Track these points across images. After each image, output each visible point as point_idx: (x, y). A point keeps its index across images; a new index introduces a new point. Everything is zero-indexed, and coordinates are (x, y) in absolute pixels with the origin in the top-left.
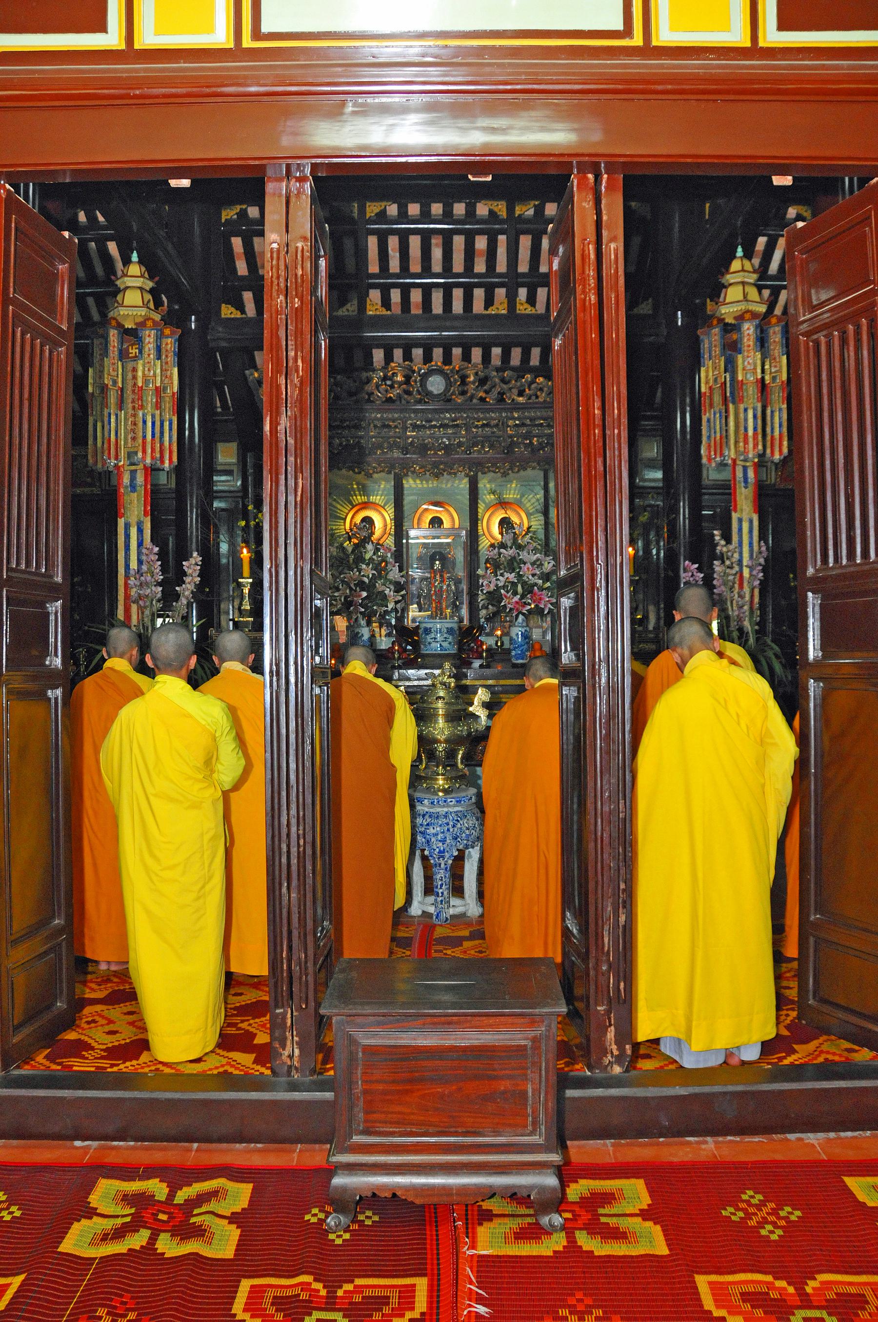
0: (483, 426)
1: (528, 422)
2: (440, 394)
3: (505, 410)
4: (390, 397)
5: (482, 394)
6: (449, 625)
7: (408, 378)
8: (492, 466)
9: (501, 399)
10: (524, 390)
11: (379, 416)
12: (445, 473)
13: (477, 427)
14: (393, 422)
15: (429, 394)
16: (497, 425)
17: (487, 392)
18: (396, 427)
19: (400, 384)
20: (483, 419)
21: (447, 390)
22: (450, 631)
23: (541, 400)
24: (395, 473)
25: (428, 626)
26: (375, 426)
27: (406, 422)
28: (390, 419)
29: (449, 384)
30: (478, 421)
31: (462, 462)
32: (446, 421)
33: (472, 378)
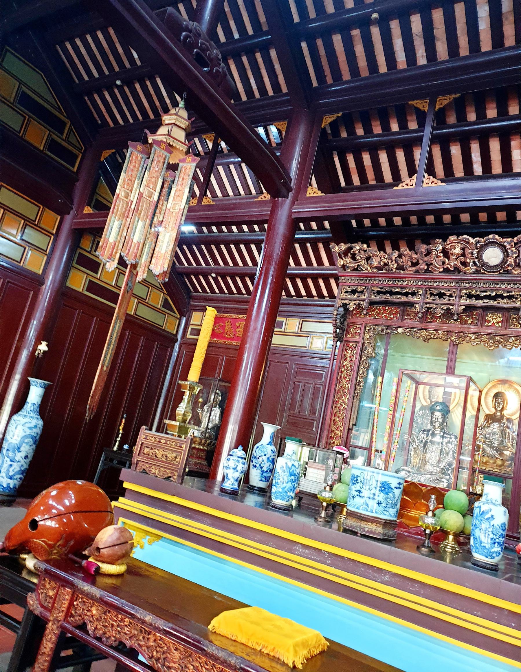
2: (497, 266)
4: (448, 268)
11: (435, 284)
12: (500, 346)
15: (484, 265)
18: (451, 296)
21: (504, 261)
26: (432, 294)
27: (461, 291)
29: (506, 254)
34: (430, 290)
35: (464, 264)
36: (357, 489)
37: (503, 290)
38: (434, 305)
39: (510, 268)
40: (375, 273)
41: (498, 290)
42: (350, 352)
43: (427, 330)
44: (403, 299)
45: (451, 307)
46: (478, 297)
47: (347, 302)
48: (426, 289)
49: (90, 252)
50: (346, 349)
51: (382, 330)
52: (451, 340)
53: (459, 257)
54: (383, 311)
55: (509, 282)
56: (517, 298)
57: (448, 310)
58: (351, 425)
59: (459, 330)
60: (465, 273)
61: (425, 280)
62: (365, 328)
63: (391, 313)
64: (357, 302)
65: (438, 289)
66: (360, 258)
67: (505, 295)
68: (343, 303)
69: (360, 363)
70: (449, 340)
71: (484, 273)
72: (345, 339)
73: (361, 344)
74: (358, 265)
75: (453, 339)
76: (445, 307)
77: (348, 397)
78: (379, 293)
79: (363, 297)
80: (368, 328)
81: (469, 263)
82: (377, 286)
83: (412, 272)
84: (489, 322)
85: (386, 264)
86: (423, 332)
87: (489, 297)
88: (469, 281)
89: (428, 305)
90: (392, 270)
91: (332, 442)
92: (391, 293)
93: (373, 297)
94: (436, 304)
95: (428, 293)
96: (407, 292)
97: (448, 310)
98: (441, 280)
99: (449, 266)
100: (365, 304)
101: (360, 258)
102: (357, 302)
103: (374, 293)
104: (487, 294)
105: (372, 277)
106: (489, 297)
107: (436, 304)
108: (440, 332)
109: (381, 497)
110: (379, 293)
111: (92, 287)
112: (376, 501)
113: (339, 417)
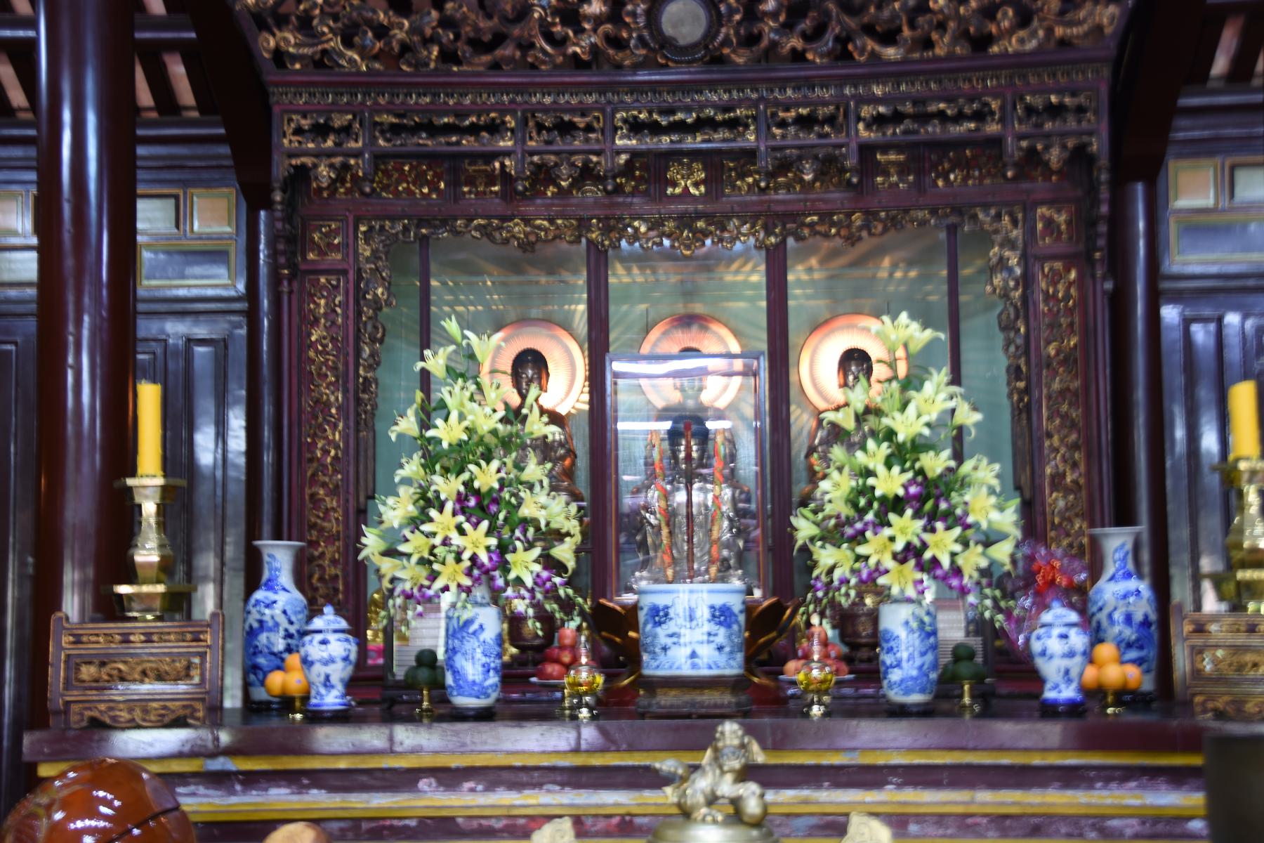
1: (908, 108)
2: (694, 47)
3: (854, 80)
4: (575, 54)
5: (796, 42)
6: (719, 600)
8: (821, 221)
9: (842, 55)
10: (900, 30)
11: (548, 100)
13: (783, 124)
14: (583, 115)
15: (666, 43)
16: (831, 120)
17: (806, 37)
18: (589, 128)
19: (598, 20)
20: (798, 104)
21: (710, 34)
22: (721, 615)
23: (940, 51)
24: (589, 242)
25: (661, 601)
26: (540, 127)
28: (573, 110)
30: (787, 110)
31: (748, 215)
32: (710, 112)
34: (533, 116)
36: (670, 632)
37: (715, 106)
38: (553, 158)
39: (726, 51)
40: (378, 73)
41: (702, 107)
42: (323, 302)
43: (527, 222)
44: (467, 143)
45: (594, 159)
46: (656, 129)
47: (308, 161)
48: (524, 112)
50: (312, 296)
51: (406, 229)
52: (589, 242)
53: (602, 23)
54: (396, 175)
55: (727, 85)
56: (747, 127)
57: (586, 163)
58: (362, 499)
59: (608, 212)
60: (619, 67)
61: (519, 89)
62: (356, 229)
63: (420, 180)
64: (338, 160)
65: (555, 110)
66: (325, 30)
67: (719, 117)
68: (296, 167)
69: (359, 330)
70: (584, 240)
71: (666, 66)
72: (303, 267)
73: (351, 276)
74: (324, 52)
75: (594, 236)
76: (578, 160)
77: (341, 426)
78: (395, 130)
79: (352, 144)
80: (363, 229)
81: (628, 41)
82: (389, 112)
83: (481, 69)
84: (674, 184)
85: (405, 48)
86: (517, 224)
87: (680, 127)
89: (536, 158)
90: (427, 65)
91: (316, 553)
92: (434, 130)
93: (381, 142)
94: (556, 153)
95: (531, 124)
96: (472, 124)
97: (586, 163)
98: (561, 88)
99: (578, 50)
100: (360, 166)
101: (325, 30)
102: (338, 160)
103: (383, 132)
104: (677, 118)
105: (368, 84)
106: (680, 127)
107: (556, 153)
108: (559, 222)
109: (721, 635)
110: (395, 130)
112: (713, 646)
113: (324, 485)
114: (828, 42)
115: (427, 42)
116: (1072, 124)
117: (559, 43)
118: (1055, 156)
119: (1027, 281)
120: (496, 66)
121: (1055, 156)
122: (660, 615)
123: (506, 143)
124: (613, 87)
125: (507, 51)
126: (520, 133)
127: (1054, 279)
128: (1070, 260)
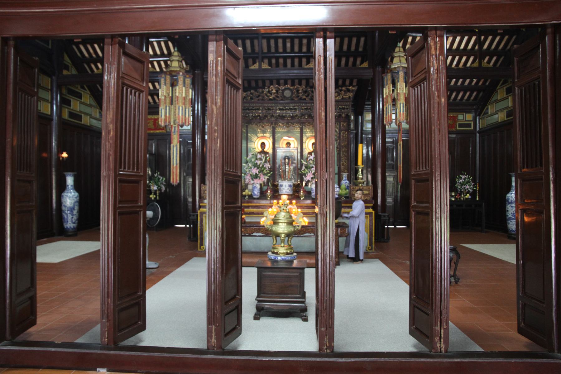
0: (305, 109)
2: (288, 98)
5: (305, 97)
7: (277, 91)
15: (285, 97)
19: (274, 93)
22: (290, 186)
29: (293, 93)
31: (298, 123)
33: (301, 91)
35: (277, 97)
46: (283, 109)
49: (66, 95)
55: (294, 103)
61: (262, 103)
88: (280, 103)
98: (269, 103)
109: (290, 188)
111: (72, 115)
114: (309, 97)
115: (248, 96)
116: (346, 111)
117: (269, 97)
118: (343, 115)
119: (340, 134)
120: (259, 100)
121: (343, 115)
122: (282, 186)
123: (260, 112)
124: (277, 103)
125: (260, 98)
126: (262, 110)
127: (343, 133)
128: (346, 131)
